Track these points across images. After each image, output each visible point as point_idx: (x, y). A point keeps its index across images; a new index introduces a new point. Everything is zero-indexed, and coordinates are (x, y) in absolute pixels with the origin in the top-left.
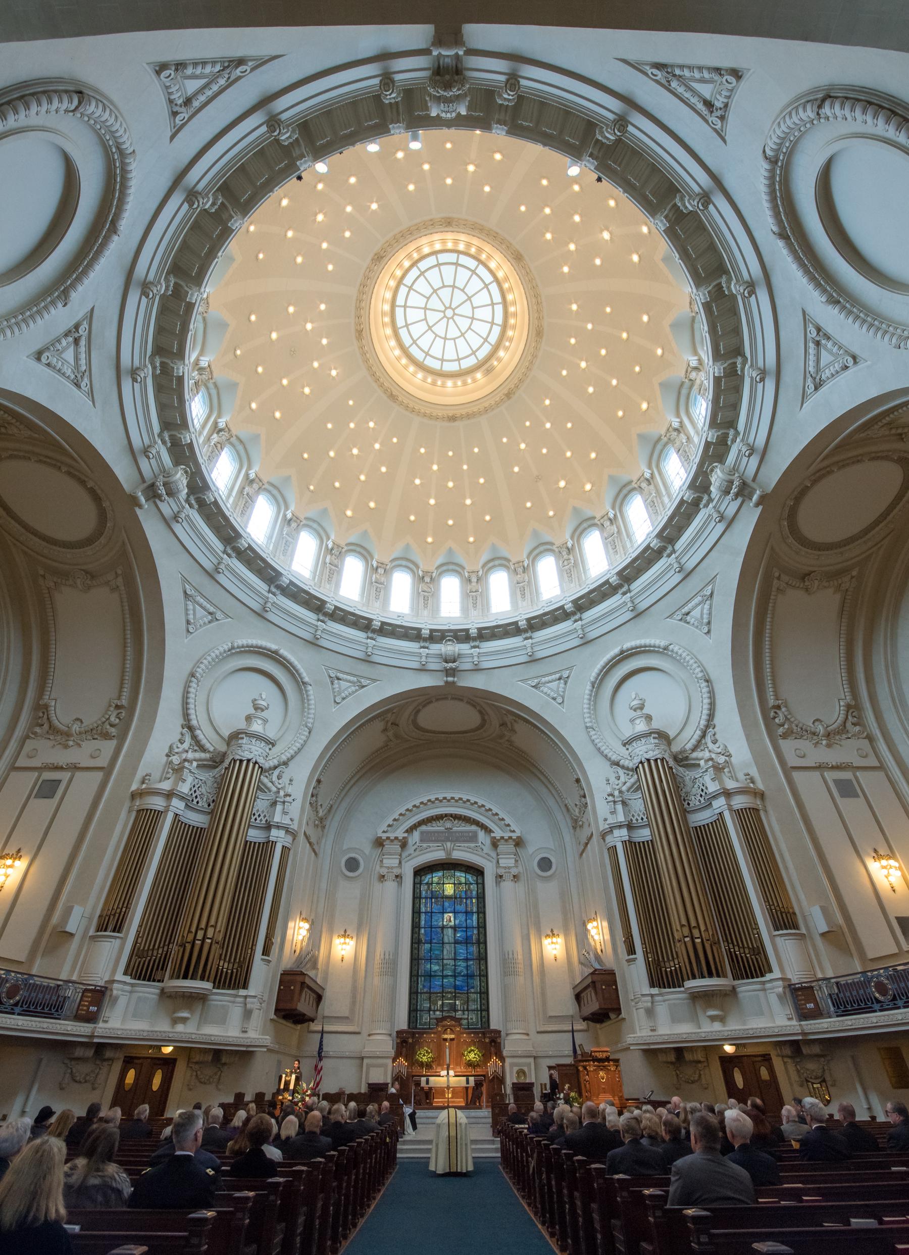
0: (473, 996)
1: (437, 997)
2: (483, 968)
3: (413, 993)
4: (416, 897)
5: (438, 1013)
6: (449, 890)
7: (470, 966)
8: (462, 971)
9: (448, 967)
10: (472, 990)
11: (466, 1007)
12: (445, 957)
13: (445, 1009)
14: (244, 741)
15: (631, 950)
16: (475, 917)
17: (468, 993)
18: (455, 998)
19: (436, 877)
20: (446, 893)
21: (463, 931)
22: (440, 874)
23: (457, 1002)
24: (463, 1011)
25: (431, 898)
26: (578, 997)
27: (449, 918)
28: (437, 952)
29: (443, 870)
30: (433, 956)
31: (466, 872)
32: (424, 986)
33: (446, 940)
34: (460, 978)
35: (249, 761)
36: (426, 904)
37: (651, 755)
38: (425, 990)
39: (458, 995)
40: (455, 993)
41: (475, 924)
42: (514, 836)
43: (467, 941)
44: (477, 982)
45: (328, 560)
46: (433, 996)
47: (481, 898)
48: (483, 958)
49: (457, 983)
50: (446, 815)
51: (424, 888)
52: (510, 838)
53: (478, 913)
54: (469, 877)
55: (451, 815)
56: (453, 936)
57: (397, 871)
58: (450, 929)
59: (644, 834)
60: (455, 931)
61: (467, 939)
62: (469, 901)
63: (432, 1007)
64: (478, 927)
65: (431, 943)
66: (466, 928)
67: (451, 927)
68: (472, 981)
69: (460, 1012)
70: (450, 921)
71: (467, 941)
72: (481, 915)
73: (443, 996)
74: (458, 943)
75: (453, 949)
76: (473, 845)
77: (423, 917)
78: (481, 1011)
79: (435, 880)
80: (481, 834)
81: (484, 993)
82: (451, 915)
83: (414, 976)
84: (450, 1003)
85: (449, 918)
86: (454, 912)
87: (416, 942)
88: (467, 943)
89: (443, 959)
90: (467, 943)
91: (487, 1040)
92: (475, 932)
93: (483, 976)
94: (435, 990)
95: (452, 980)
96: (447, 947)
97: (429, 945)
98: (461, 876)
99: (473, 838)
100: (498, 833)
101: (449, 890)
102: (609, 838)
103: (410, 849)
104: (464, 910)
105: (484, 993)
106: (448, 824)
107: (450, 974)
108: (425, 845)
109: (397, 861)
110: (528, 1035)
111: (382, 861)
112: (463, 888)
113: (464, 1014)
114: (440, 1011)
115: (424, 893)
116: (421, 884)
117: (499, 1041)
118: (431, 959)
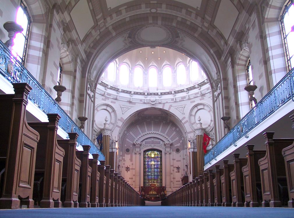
0: (158, 180)
3: (144, 179)
4: (144, 158)
6: (153, 156)
14: (106, 131)
15: (191, 174)
16: (159, 162)
18: (154, 180)
19: (149, 153)
20: (152, 157)
22: (150, 152)
25: (148, 158)
26: (182, 181)
27: (153, 163)
29: (151, 151)
31: (157, 151)
33: (152, 168)
35: (107, 135)
36: (147, 159)
37: (199, 134)
41: (159, 164)
42: (170, 143)
43: (157, 168)
44: (159, 177)
45: (117, 72)
46: (149, 180)
47: (161, 158)
48: (161, 172)
50: (152, 137)
51: (146, 155)
52: (169, 144)
53: (160, 161)
54: (158, 152)
55: (153, 137)
57: (139, 152)
59: (196, 150)
62: (158, 159)
64: (160, 165)
65: (148, 168)
71: (157, 168)
72: (161, 162)
76: (159, 145)
77: (146, 162)
78: (160, 183)
79: (149, 153)
80: (161, 142)
81: (161, 180)
82: (154, 162)
83: (144, 176)
85: (153, 163)
86: (154, 161)
87: (144, 168)
92: (159, 166)
95: (153, 176)
96: (152, 169)
98: (156, 153)
99: (160, 143)
100: (167, 142)
101: (153, 156)
102: (189, 150)
103: (142, 146)
106: (152, 139)
108: (146, 145)
109: (139, 150)
110: (171, 188)
111: (135, 149)
112: (157, 155)
115: (146, 156)
116: (145, 154)
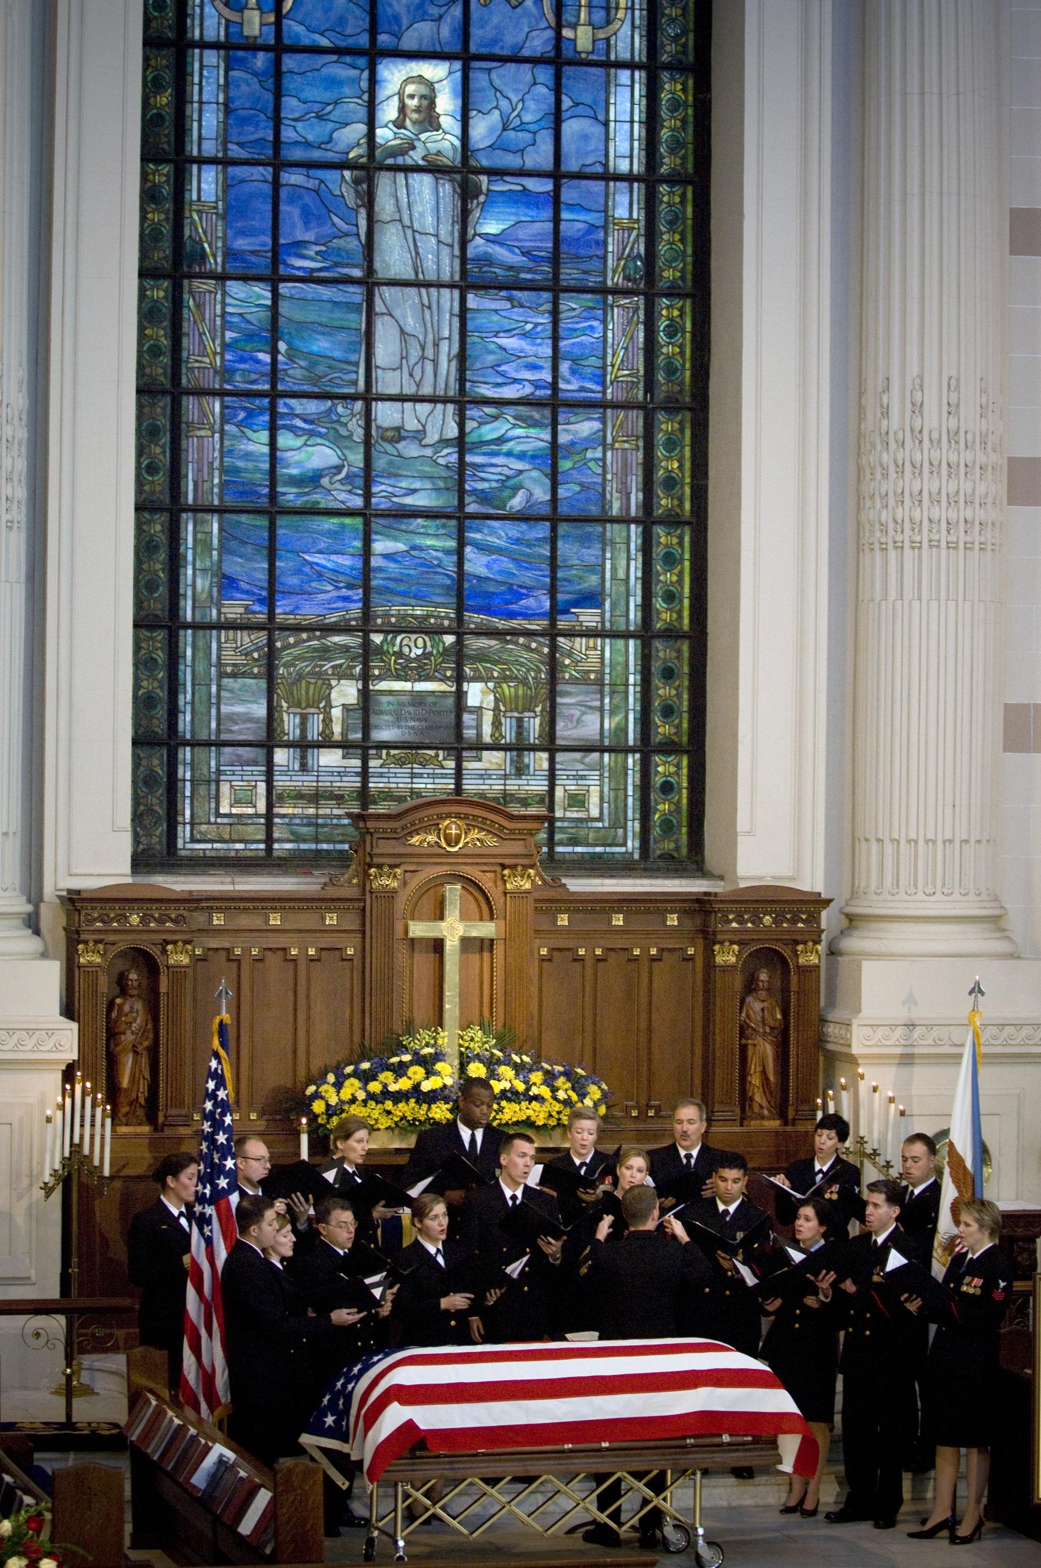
1: (325, 653)
2: (668, 465)
5: (330, 758)
7: (576, 448)
8: (510, 485)
9: (410, 449)
10: (589, 617)
11: (534, 726)
12: (388, 382)
13: (384, 734)
17: (552, 634)
21: (526, 198)
23: (476, 693)
24: (519, 748)
28: (321, 345)
30: (294, 376)
32: (227, 584)
34: (499, 534)
38: (233, 609)
39: (476, 644)
40: (459, 630)
49: (476, 564)
56: (448, 231)
58: (423, 183)
60: (467, 193)
61: (555, 259)
63: (290, 724)
65: (274, 280)
66: (557, 175)
67: (433, 168)
68: (591, 554)
69: (493, 759)
70: (430, 120)
73: (368, 651)
74: (485, 287)
75: (449, 327)
78: (647, 748)
82: (434, 71)
84: (418, 699)
88: (556, 288)
89: (369, 397)
90: (556, 288)
91: (727, 956)
93: (673, 521)
94: (309, 612)
97: (261, 293)
104: (539, 43)
105: (671, 634)
107: (420, 501)
113: (520, 770)
114: (345, 745)
117: (809, 958)
118: (274, 395)
